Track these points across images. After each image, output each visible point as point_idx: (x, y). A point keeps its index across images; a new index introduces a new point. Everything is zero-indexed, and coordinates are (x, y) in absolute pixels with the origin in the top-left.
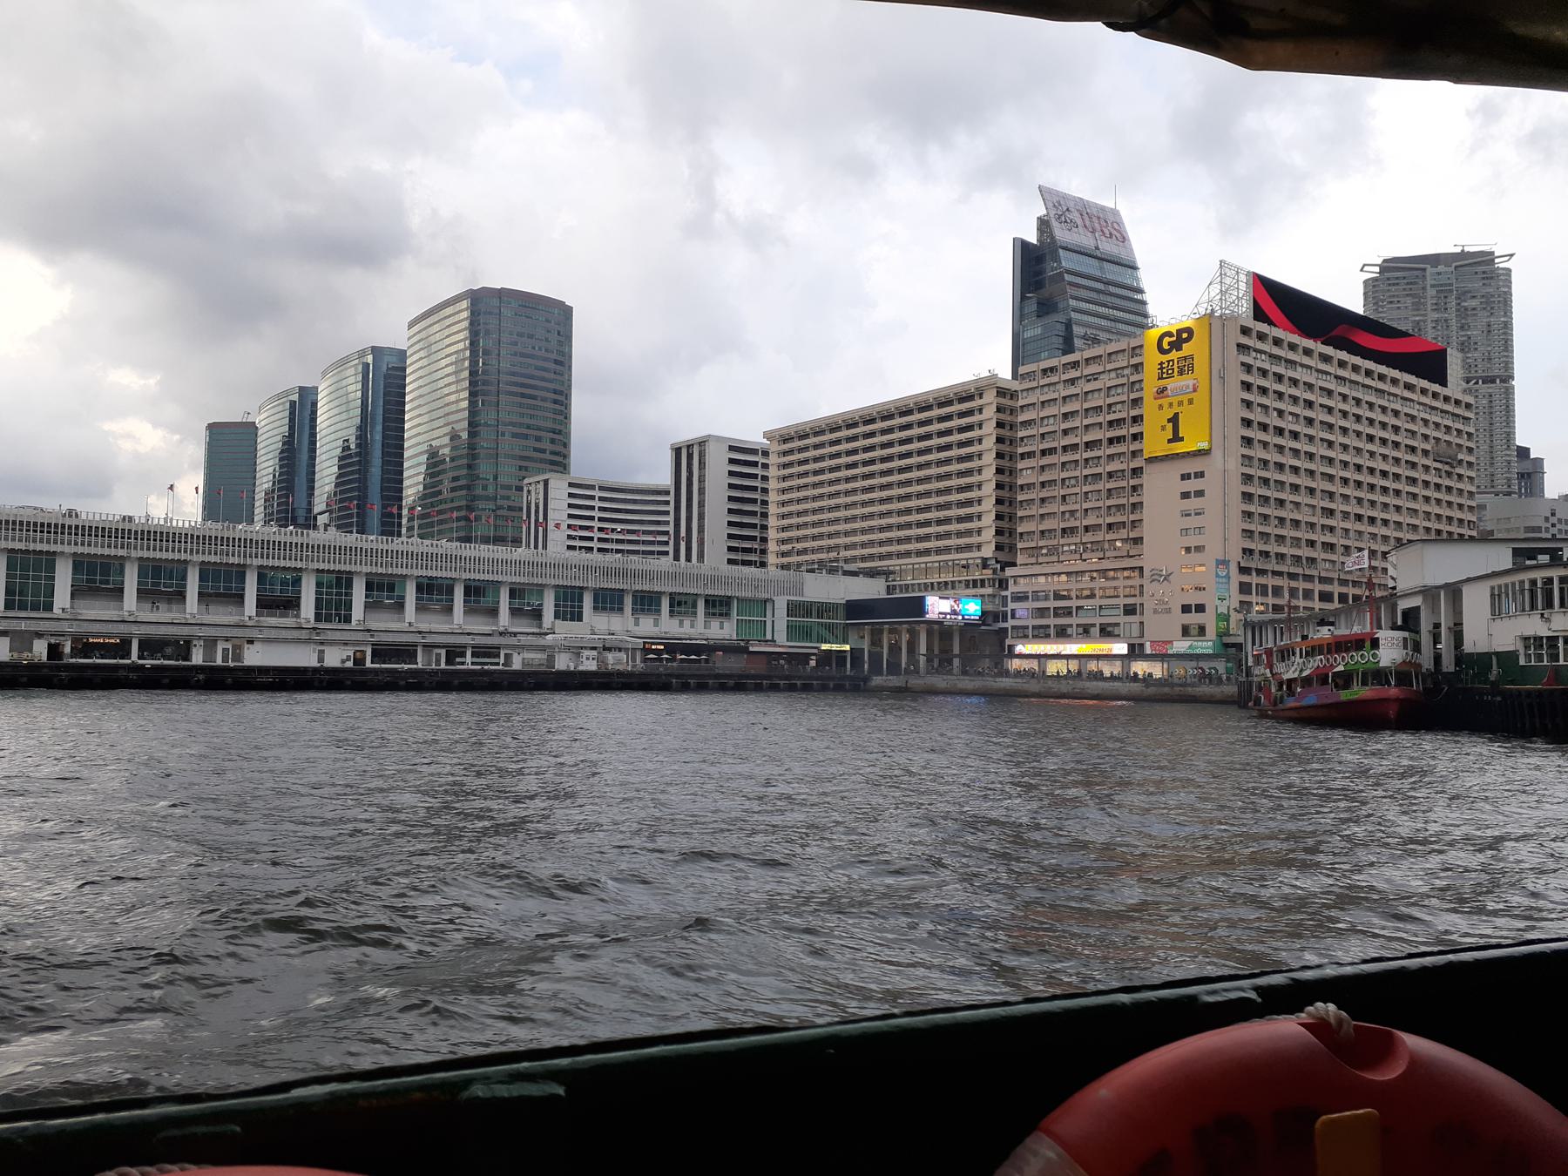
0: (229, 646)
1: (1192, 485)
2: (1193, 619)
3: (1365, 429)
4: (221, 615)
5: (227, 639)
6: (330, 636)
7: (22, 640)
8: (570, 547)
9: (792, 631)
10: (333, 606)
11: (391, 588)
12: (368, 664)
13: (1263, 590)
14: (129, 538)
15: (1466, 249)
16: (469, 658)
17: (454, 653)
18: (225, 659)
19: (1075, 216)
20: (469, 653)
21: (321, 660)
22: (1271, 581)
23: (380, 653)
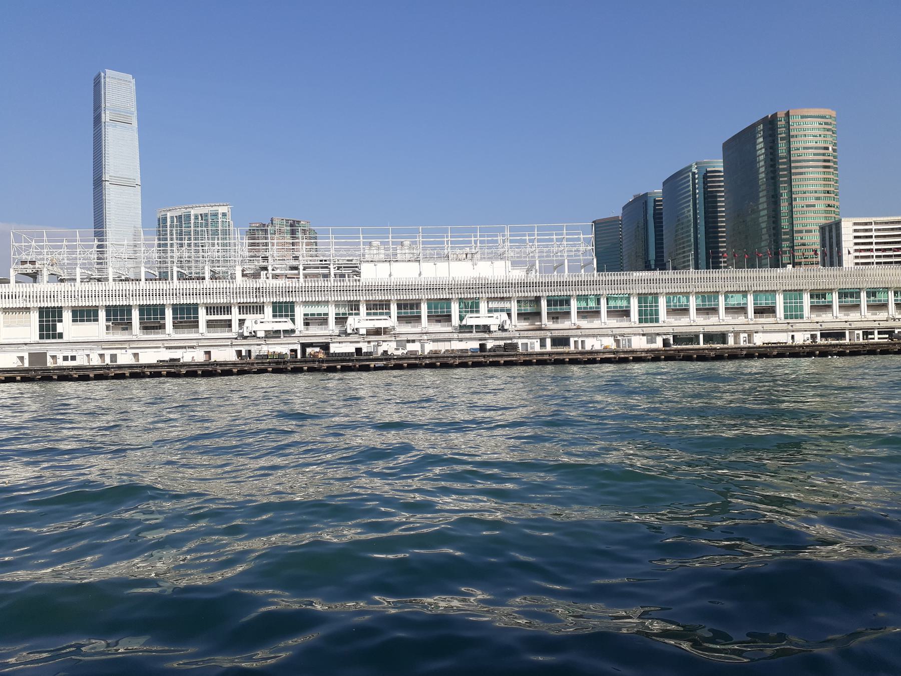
0: (746, 335)
5: (745, 332)
6: (795, 327)
7: (651, 338)
8: (857, 264)
11: (824, 296)
16: (876, 336)
17: (867, 333)
20: (876, 332)
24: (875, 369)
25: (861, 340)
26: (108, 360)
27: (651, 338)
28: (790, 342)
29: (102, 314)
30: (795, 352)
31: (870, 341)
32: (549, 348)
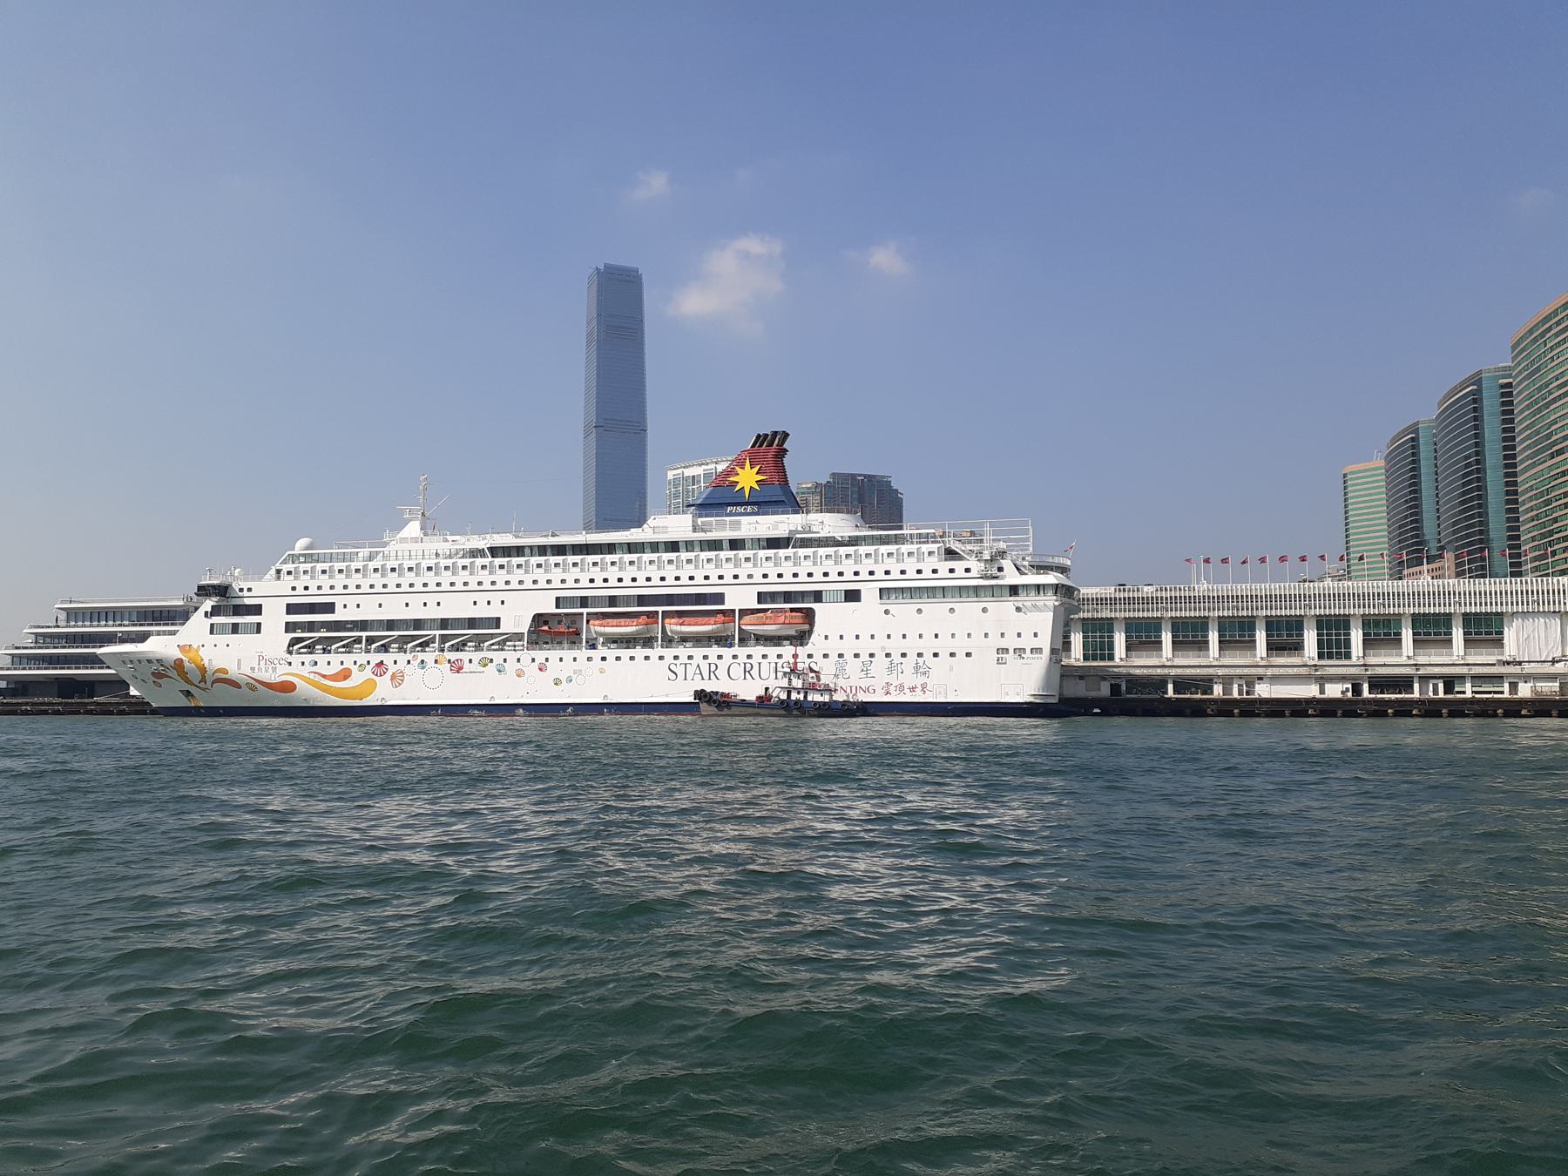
0: (1243, 682)
4: (1236, 659)
10: (1332, 644)
12: (1366, 694)
14: (1162, 603)
17: (1450, 682)
18: (1240, 693)
21: (1322, 691)
23: (1378, 683)
25: (1441, 695)
28: (1318, 695)
30: (1326, 709)
31: (1458, 696)
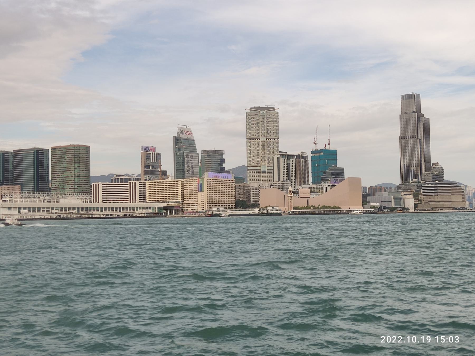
1: (202, 195)
2: (203, 208)
3: (220, 186)
7: (103, 215)
9: (158, 211)
13: (209, 205)
15: (269, 107)
19: (184, 132)
22: (210, 204)
24: (90, 227)
26: (50, 217)
27: (103, 215)
29: (27, 209)
32: (90, 217)
